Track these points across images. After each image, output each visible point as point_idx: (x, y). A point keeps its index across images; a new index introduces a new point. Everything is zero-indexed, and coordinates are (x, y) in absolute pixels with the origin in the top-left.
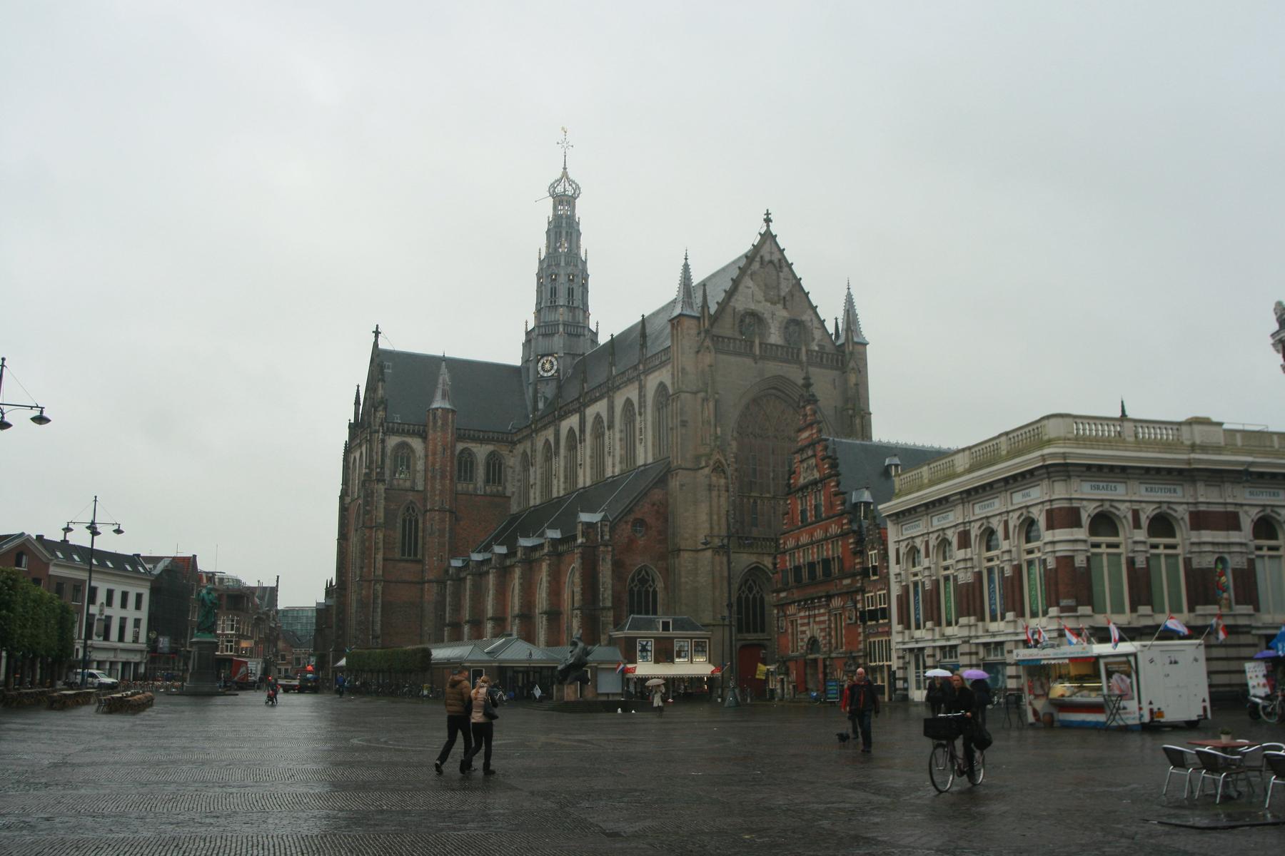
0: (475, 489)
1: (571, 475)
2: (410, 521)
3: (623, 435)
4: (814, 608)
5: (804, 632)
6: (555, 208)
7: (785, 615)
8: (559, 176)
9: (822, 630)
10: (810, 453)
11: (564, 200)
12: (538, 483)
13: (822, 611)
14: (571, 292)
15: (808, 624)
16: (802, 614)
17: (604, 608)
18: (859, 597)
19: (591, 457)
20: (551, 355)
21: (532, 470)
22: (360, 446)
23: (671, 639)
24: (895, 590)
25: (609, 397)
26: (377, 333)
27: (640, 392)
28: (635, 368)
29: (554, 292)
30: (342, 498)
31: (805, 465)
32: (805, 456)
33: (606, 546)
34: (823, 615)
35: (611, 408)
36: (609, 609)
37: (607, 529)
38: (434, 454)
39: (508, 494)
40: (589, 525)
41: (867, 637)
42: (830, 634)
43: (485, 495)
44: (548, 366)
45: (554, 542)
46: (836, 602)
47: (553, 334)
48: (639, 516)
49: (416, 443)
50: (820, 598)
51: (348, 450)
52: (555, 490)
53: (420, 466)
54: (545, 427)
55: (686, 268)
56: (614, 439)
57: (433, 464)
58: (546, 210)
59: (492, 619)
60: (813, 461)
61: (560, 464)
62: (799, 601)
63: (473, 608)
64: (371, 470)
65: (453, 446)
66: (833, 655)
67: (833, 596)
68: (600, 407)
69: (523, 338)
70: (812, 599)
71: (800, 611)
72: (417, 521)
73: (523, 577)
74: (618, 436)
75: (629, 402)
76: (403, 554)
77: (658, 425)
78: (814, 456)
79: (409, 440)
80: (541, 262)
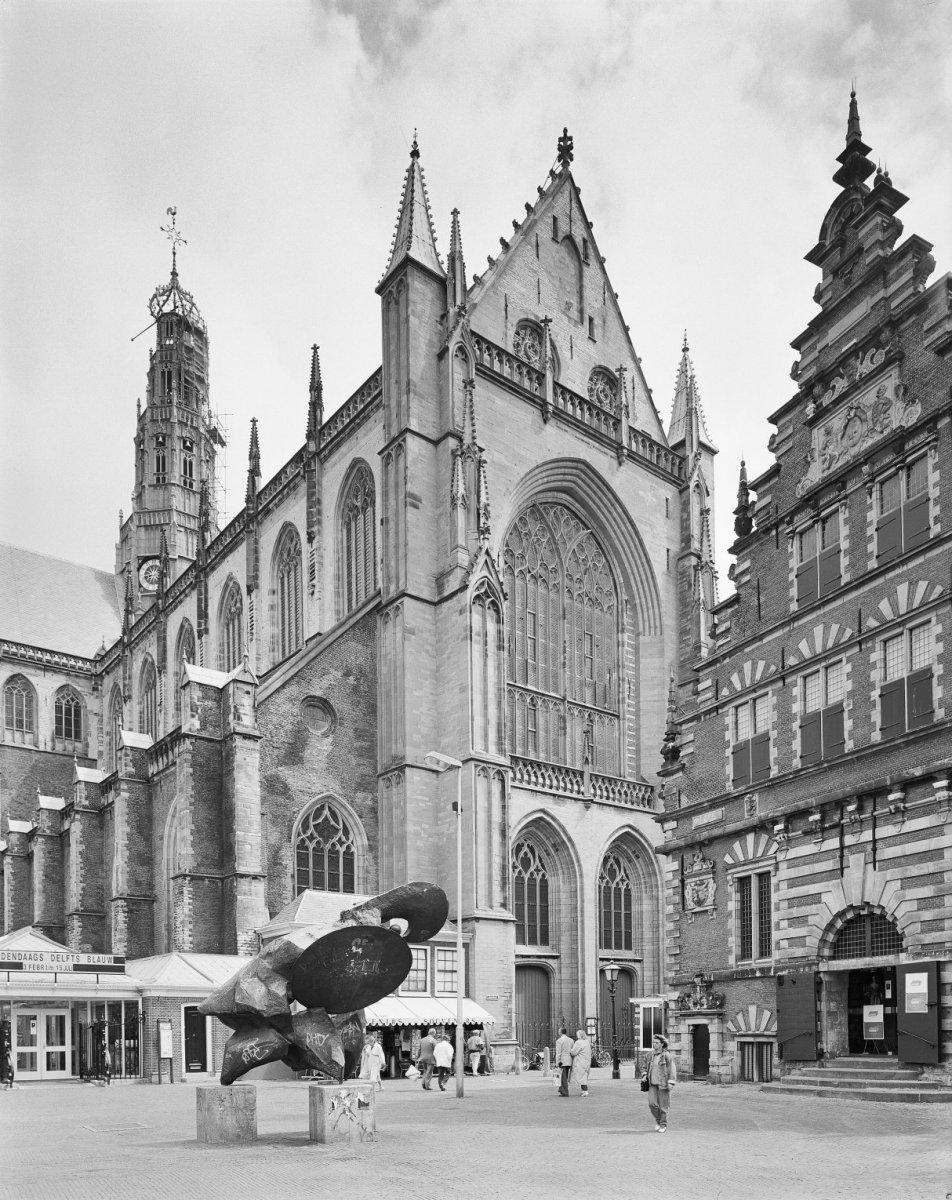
29: (161, 464)
48: (318, 693)
62: (791, 818)
71: (790, 842)
75: (288, 530)
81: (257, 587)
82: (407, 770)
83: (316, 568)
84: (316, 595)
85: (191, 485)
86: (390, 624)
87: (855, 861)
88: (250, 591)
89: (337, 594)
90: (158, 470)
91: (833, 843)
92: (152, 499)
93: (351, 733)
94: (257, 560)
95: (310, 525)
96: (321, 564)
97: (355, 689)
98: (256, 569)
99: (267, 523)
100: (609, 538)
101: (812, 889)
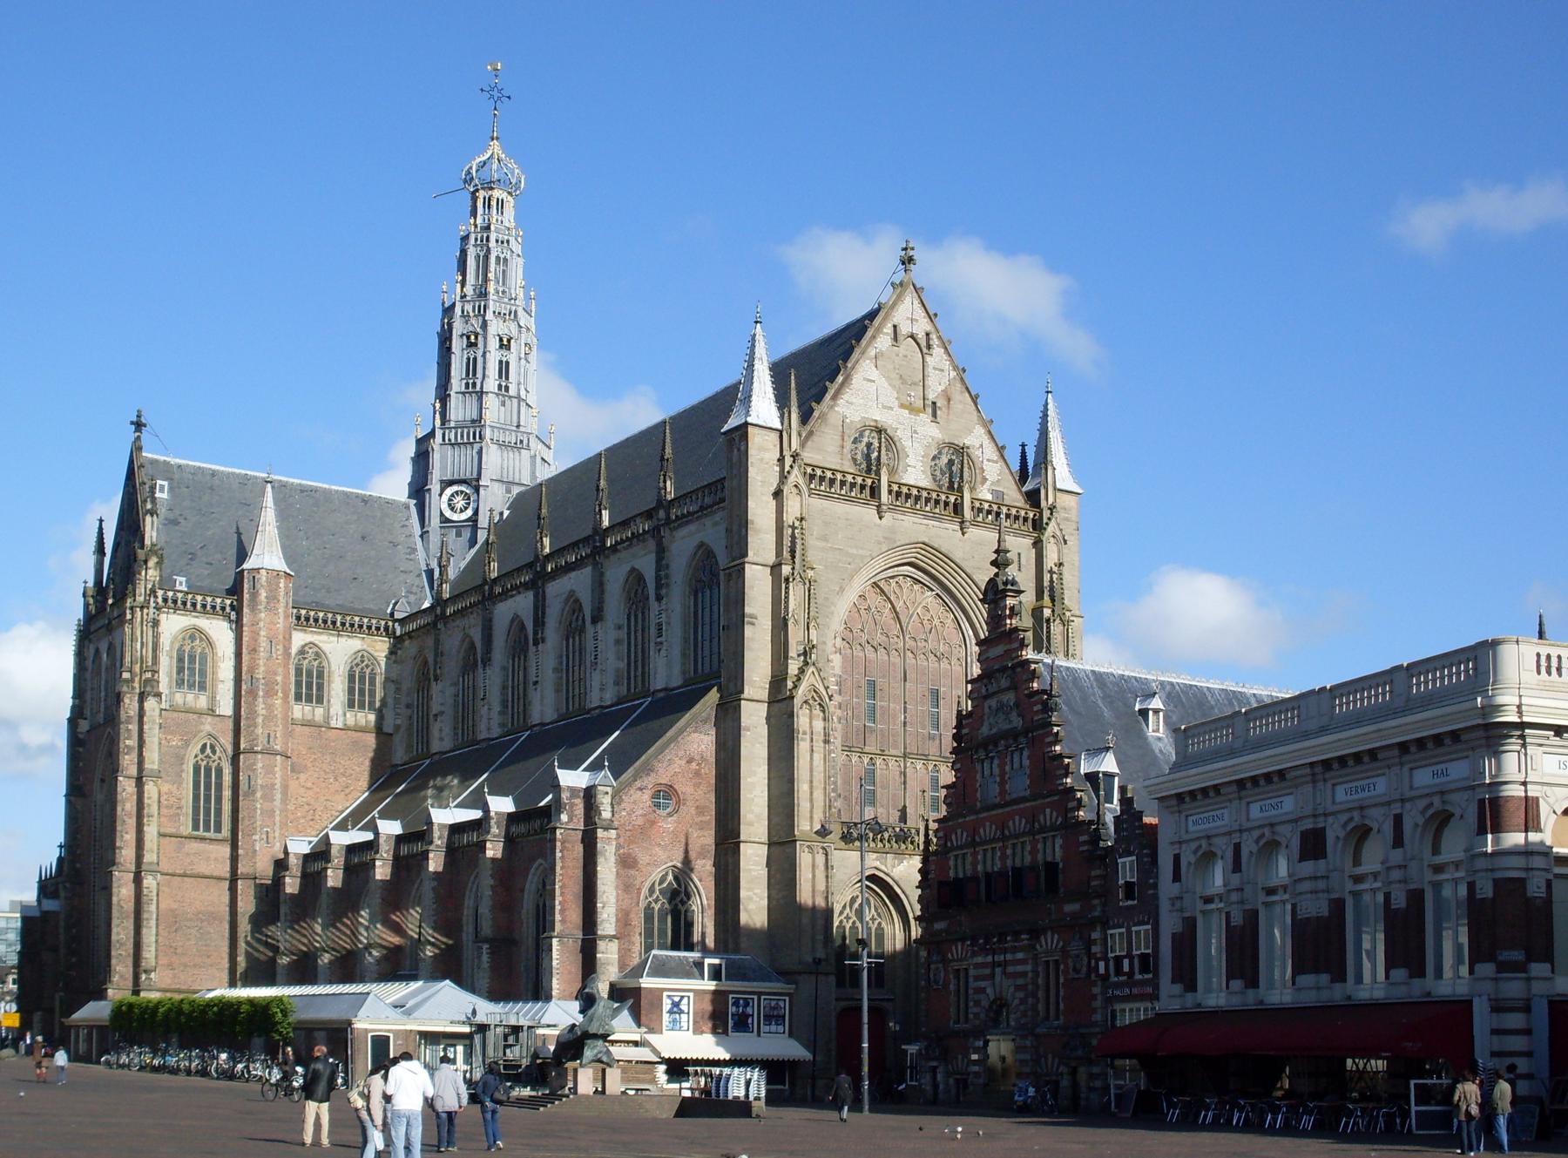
0: (327, 717)
1: (517, 696)
3: (623, 634)
4: (1005, 951)
5: (983, 990)
7: (945, 961)
9: (1018, 988)
10: (1004, 683)
13: (1020, 955)
15: (992, 976)
16: (979, 959)
18: (1095, 935)
19: (556, 670)
21: (436, 688)
24: (1169, 924)
25: (595, 564)
27: (659, 559)
29: (471, 367)
30: (73, 722)
31: (993, 702)
32: (991, 690)
34: (1023, 962)
35: (599, 585)
38: (254, 650)
41: (1109, 1001)
42: (1034, 995)
43: (346, 728)
44: (459, 502)
46: (1050, 941)
49: (220, 632)
50: (1017, 934)
52: (482, 726)
53: (226, 670)
56: (606, 640)
57: (252, 670)
60: (1010, 698)
61: (492, 680)
65: (288, 639)
66: (1038, 1030)
67: (1044, 931)
70: (1002, 937)
71: (974, 954)
72: (219, 771)
74: (612, 635)
75: (636, 577)
77: (694, 621)
78: (1014, 687)
84: (663, 653)
85: (507, 389)
87: (998, 970)
88: (595, 620)
89: (684, 655)
91: (990, 959)
93: (693, 810)
94: (602, 592)
95: (658, 579)
96: (668, 624)
97: (697, 774)
98: (601, 601)
99: (613, 558)
101: (982, 984)
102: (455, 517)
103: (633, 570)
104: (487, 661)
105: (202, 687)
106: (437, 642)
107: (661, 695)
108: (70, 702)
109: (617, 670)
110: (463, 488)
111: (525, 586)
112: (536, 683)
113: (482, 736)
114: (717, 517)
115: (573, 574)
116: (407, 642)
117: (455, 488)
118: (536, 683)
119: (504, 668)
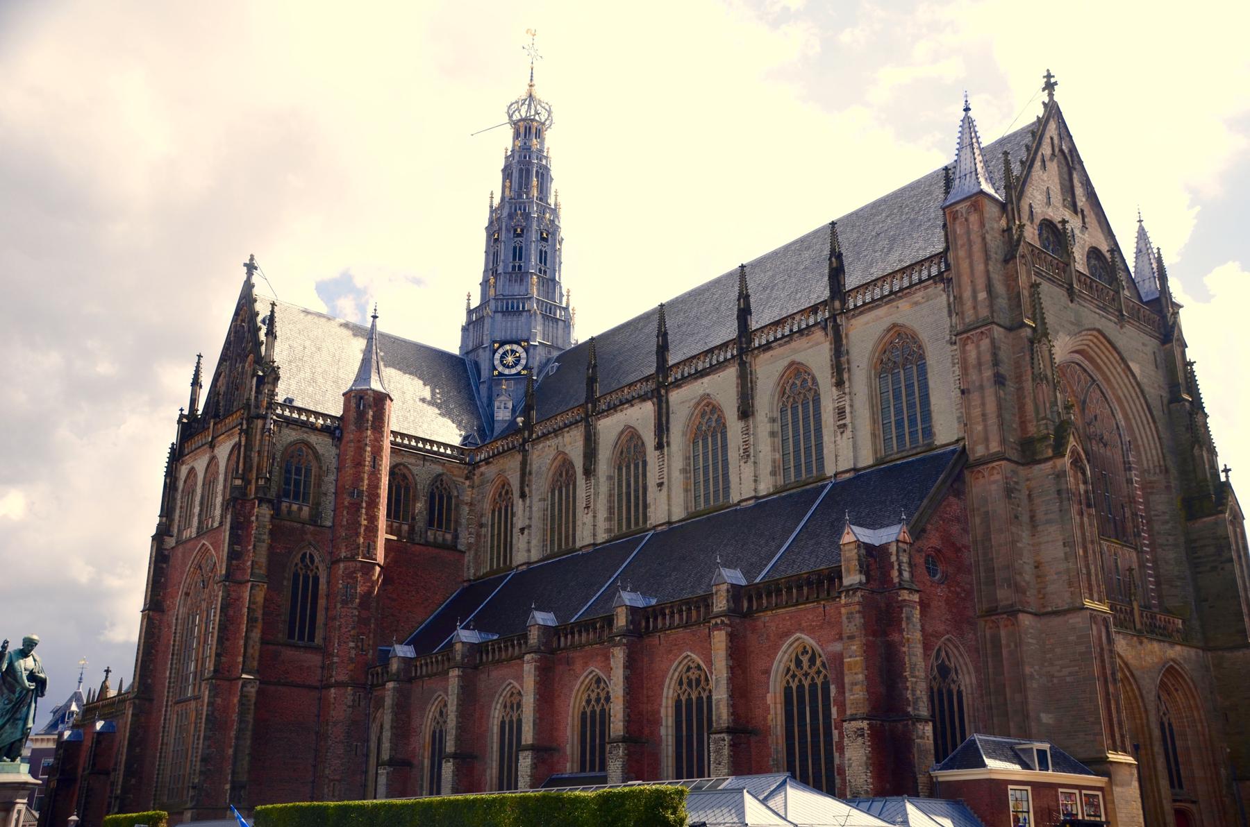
2: (306, 578)
6: (517, 135)
8: (522, 93)
11: (528, 131)
12: (536, 523)
14: (543, 257)
17: (919, 719)
19: (684, 471)
20: (518, 343)
22: (212, 446)
23: (1053, 786)
25: (742, 364)
26: (251, 267)
28: (814, 309)
29: (518, 253)
30: (159, 538)
33: (911, 591)
36: (926, 721)
37: (905, 559)
39: (459, 547)
40: (869, 548)
44: (510, 359)
45: (736, 592)
47: (518, 313)
51: (176, 456)
54: (557, 432)
55: (968, 125)
58: (505, 140)
59: (531, 748)
63: (462, 728)
64: (247, 482)
68: (722, 386)
69: (463, 320)
72: (316, 579)
73: (631, 664)
75: (797, 370)
76: (291, 636)
79: (313, 439)
80: (492, 211)
81: (753, 414)
82: (1021, 616)
83: (848, 410)
84: (848, 433)
86: (982, 481)
90: (514, 259)
92: (504, 287)
99: (764, 357)
100: (1113, 388)
102: (507, 372)
103: (792, 363)
104: (589, 472)
105: (305, 500)
106: (524, 464)
107: (847, 476)
108: (157, 520)
109: (774, 461)
110: (515, 347)
111: (643, 398)
112: (660, 485)
113: (586, 542)
114: (918, 296)
115: (706, 380)
116: (482, 469)
117: (508, 347)
118: (660, 485)
119: (610, 478)
